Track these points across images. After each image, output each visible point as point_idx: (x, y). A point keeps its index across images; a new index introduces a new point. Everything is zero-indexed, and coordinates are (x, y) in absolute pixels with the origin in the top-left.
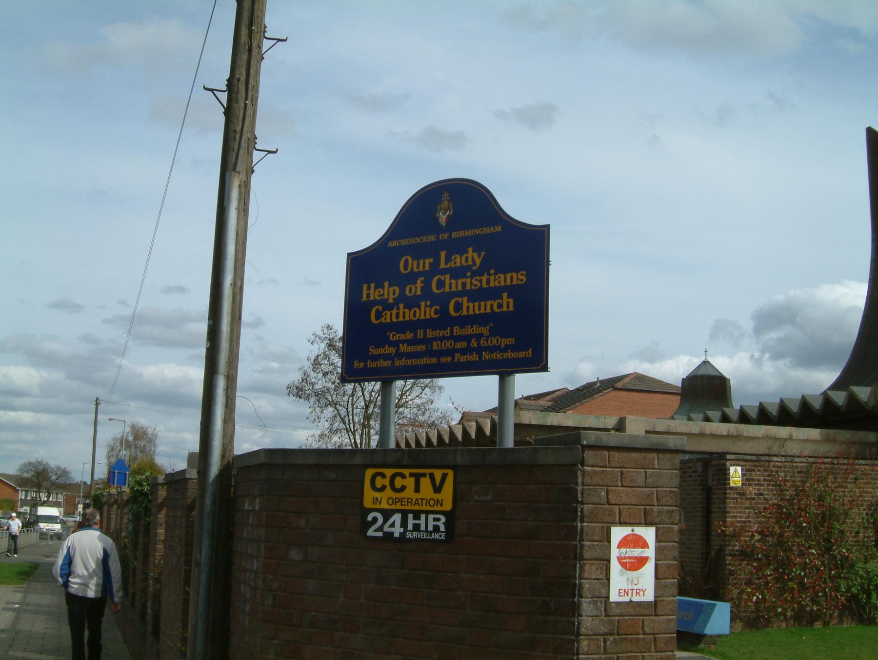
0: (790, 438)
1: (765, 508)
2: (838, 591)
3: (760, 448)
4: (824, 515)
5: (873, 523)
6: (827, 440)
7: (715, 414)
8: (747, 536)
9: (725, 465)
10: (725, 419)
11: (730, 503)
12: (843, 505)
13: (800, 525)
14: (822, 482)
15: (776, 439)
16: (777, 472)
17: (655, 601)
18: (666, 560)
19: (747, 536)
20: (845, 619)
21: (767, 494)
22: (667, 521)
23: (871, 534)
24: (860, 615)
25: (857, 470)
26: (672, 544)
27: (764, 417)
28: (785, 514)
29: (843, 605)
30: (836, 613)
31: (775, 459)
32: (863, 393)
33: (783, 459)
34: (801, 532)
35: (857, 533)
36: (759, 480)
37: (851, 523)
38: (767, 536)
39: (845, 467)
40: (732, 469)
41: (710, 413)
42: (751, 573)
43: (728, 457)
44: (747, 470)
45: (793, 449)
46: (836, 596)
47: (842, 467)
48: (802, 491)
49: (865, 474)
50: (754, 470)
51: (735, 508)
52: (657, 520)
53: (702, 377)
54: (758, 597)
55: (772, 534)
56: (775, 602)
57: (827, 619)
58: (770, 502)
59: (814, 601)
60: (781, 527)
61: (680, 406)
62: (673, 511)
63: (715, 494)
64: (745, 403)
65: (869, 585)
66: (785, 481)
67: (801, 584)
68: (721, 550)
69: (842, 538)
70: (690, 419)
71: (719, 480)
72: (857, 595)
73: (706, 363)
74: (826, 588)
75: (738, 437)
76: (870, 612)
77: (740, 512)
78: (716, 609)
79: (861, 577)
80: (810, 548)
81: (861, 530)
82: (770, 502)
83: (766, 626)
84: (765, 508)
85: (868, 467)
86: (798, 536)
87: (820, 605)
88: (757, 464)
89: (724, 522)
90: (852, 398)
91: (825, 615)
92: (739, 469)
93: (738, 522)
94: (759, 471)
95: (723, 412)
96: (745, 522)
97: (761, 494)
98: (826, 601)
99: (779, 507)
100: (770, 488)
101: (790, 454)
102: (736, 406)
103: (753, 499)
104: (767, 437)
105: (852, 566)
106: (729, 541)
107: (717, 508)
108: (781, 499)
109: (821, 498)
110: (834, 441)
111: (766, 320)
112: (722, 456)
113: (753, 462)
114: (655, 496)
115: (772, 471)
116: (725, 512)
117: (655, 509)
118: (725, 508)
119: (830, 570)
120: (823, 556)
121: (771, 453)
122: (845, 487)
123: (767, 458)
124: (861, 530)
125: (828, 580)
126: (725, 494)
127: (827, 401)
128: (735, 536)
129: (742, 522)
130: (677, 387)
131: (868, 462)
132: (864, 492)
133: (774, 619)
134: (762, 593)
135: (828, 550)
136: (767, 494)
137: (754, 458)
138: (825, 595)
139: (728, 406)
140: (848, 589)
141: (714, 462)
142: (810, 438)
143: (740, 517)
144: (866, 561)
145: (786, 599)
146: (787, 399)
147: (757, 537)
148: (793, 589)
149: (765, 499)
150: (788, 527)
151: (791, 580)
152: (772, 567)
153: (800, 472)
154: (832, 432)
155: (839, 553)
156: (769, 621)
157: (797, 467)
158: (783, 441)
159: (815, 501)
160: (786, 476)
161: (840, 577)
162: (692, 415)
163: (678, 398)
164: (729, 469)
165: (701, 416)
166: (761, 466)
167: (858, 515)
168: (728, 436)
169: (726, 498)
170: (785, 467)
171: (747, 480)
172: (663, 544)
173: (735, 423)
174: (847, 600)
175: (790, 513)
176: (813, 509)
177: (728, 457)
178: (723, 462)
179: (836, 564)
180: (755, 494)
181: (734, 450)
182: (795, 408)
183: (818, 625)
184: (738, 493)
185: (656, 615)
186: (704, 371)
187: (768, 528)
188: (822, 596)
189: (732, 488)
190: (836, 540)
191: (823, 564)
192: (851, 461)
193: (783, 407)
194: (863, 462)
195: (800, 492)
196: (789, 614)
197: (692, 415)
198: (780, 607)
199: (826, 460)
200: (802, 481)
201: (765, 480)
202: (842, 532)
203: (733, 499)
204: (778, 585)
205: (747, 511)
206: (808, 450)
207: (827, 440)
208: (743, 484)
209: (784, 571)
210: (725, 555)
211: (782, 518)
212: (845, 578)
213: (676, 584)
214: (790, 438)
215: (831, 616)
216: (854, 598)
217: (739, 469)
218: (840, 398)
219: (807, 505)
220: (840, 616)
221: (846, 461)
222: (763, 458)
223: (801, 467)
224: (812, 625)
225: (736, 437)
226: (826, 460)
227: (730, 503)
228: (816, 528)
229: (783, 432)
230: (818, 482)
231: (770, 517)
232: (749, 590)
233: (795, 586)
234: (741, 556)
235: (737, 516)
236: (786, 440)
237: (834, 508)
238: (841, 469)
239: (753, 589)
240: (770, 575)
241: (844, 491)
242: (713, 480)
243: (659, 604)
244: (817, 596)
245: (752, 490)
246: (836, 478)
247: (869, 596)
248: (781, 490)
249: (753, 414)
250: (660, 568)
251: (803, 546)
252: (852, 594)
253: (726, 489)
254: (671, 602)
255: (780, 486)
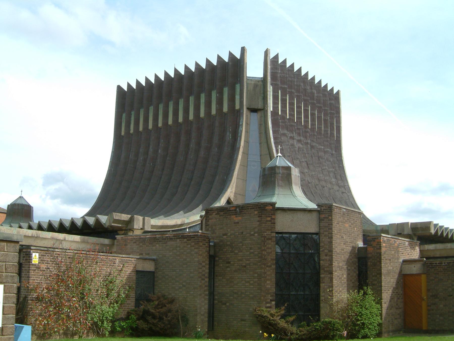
0: (65, 240)
1: (50, 276)
2: (87, 320)
3: (49, 244)
4: (81, 280)
5: (106, 285)
6: (83, 242)
7: (25, 225)
8: (40, 290)
9: (30, 252)
10: (30, 228)
11: (32, 272)
12: (91, 276)
13: (68, 286)
14: (80, 263)
15: (57, 240)
16: (57, 257)
17: (2, 327)
18: (9, 303)
19: (40, 290)
20: (90, 334)
21: (52, 269)
22: (10, 281)
23: (105, 291)
24: (98, 332)
25: (99, 258)
26: (13, 295)
27: (51, 228)
28: (61, 279)
29: (89, 327)
30: (86, 331)
31: (57, 250)
32: (103, 219)
33: (61, 250)
34: (69, 289)
35: (98, 290)
36: (47, 261)
37: (95, 285)
38: (51, 291)
39: (93, 256)
40: (34, 254)
41: (22, 224)
42: (41, 310)
43: (32, 248)
44: (42, 255)
45: (65, 245)
46: (86, 323)
47: (91, 256)
48: (70, 267)
49: (103, 260)
50: (45, 256)
51: (35, 275)
52: (4, 281)
53: (18, 204)
54: (45, 323)
55: (53, 290)
56: (53, 326)
57: (81, 334)
58: (53, 273)
59: (74, 325)
60: (58, 286)
61: (6, 219)
62: (14, 276)
63: (24, 267)
64: (41, 220)
65: (103, 317)
66: (62, 262)
67: (68, 316)
68: (26, 298)
69: (90, 293)
70: (11, 226)
71: (26, 260)
72: (97, 322)
73: (21, 197)
74: (81, 318)
75: (37, 237)
76: (103, 331)
77: (37, 277)
78: (24, 329)
79: (99, 313)
80: (73, 297)
81: (100, 289)
82: (53, 273)
83: (49, 338)
84: (50, 276)
85: (104, 257)
86: (67, 291)
87: (77, 327)
88: (47, 252)
89: (28, 282)
90: (98, 222)
91: (80, 333)
92: (37, 254)
93: (36, 282)
94: (48, 256)
95: (29, 224)
96: (39, 283)
97: (49, 268)
98: (80, 325)
99: (58, 275)
100: (54, 265)
101: (65, 248)
102: (36, 221)
103: (44, 271)
104: (52, 238)
105: (95, 307)
106: (30, 293)
107: (25, 275)
108: (59, 271)
109: (79, 272)
110: (88, 243)
111: (49, 180)
112: (29, 247)
113: (45, 251)
114: (4, 267)
115: (55, 256)
116: (29, 277)
117: (4, 274)
118: (29, 275)
119: (83, 309)
120: (79, 302)
121: (55, 246)
122: (92, 267)
123: (52, 249)
124: (100, 289)
125: (82, 314)
126: (29, 267)
127: (85, 223)
128: (35, 289)
129: (37, 283)
130: (4, 209)
131: (104, 254)
132: (101, 269)
133: (53, 335)
134: (47, 320)
135: (83, 298)
136: (52, 269)
137: (46, 249)
138: (80, 322)
139: (31, 221)
140: (92, 319)
141: (24, 250)
142: (75, 240)
143: (37, 280)
144: (102, 305)
145: (60, 324)
146: (63, 219)
147: (46, 291)
148: (64, 318)
149: (50, 271)
150: (62, 286)
151: (62, 314)
152: (53, 307)
153: (69, 258)
154: (86, 238)
155: (88, 301)
156: (50, 335)
157: (68, 255)
158: (61, 241)
159: (76, 273)
160: (62, 260)
161: (88, 313)
162: (12, 224)
163: (5, 215)
164: (32, 254)
165: (17, 225)
166: (50, 254)
167: (98, 282)
168: (32, 237)
169: (29, 270)
170: (62, 254)
171: (42, 260)
172: (7, 294)
173: (35, 230)
174: (91, 325)
175: (63, 279)
176: (75, 277)
177: (32, 248)
178: (29, 250)
179: (86, 306)
180: (45, 268)
181: (34, 245)
182: (67, 224)
183: (76, 337)
184: (36, 267)
185: (2, 335)
186: (20, 202)
187: (51, 286)
188: (79, 322)
189: (33, 265)
190: (87, 294)
191: (79, 306)
192: (97, 253)
193: (73, 223)
194: (102, 254)
195: (69, 268)
196: (61, 331)
197: (12, 224)
198: (56, 328)
199: (83, 252)
200: (70, 262)
201: (51, 261)
202: (89, 289)
203: (33, 270)
204: (55, 316)
205: (41, 277)
206: (74, 246)
207: (83, 242)
208: (39, 263)
209: (59, 309)
210: (28, 300)
211: (58, 281)
212: (90, 313)
213: (14, 317)
214: (65, 240)
215: (83, 333)
216: (95, 324)
217: (37, 254)
218: (91, 221)
219: (72, 275)
220: (88, 333)
221: (93, 253)
222: (50, 249)
223: (70, 255)
224: (73, 338)
225: (36, 237)
226: (83, 252)
227: (32, 273)
228: (76, 287)
229: (61, 236)
230: (78, 263)
231: (53, 281)
232: (40, 319)
233: (65, 317)
234: (36, 300)
235: (35, 279)
236: (62, 240)
237: (86, 277)
238: (90, 257)
239: (42, 318)
240: (52, 311)
241: (91, 269)
242: (23, 260)
243: (4, 329)
244: (76, 322)
245: (43, 266)
246: (88, 262)
247: (103, 323)
248: (59, 267)
249: (45, 226)
250: (6, 309)
251: (69, 296)
252: (94, 322)
253: (30, 265)
254: (11, 328)
255: (58, 264)
